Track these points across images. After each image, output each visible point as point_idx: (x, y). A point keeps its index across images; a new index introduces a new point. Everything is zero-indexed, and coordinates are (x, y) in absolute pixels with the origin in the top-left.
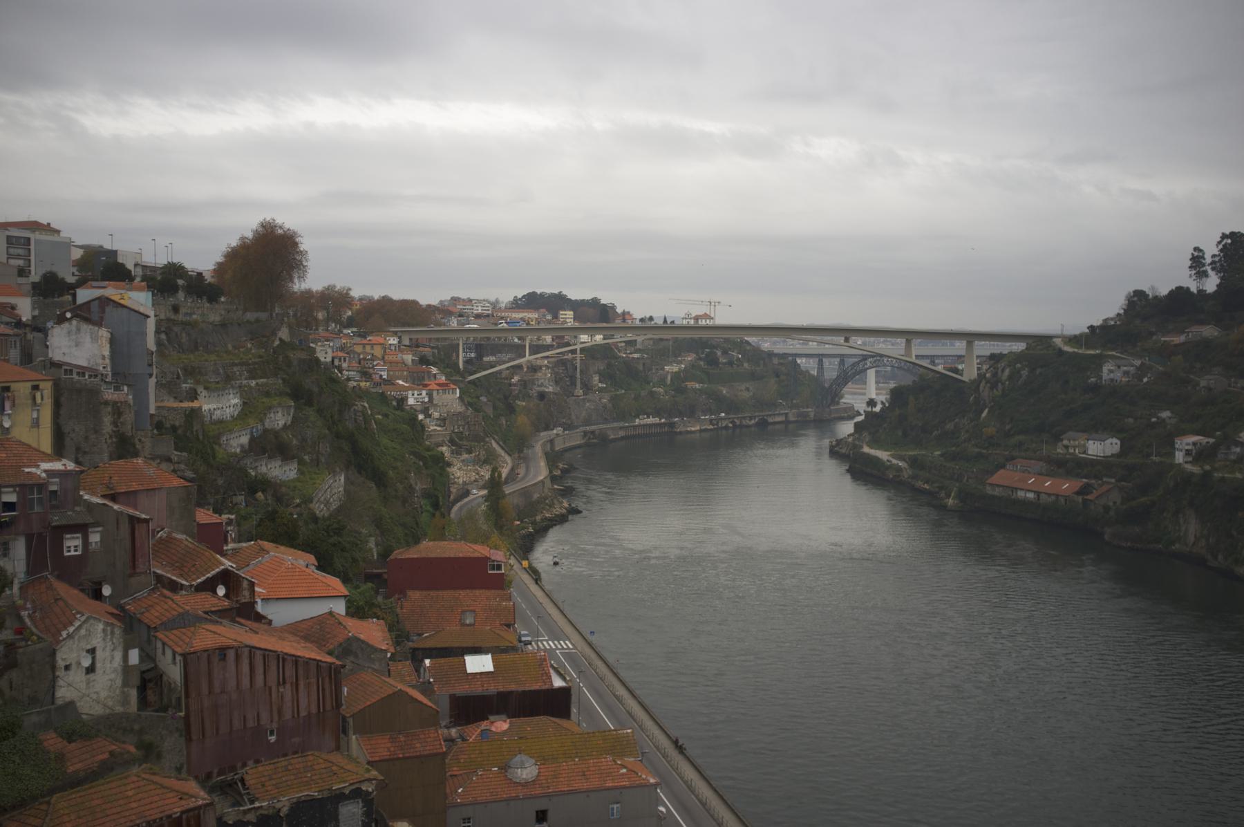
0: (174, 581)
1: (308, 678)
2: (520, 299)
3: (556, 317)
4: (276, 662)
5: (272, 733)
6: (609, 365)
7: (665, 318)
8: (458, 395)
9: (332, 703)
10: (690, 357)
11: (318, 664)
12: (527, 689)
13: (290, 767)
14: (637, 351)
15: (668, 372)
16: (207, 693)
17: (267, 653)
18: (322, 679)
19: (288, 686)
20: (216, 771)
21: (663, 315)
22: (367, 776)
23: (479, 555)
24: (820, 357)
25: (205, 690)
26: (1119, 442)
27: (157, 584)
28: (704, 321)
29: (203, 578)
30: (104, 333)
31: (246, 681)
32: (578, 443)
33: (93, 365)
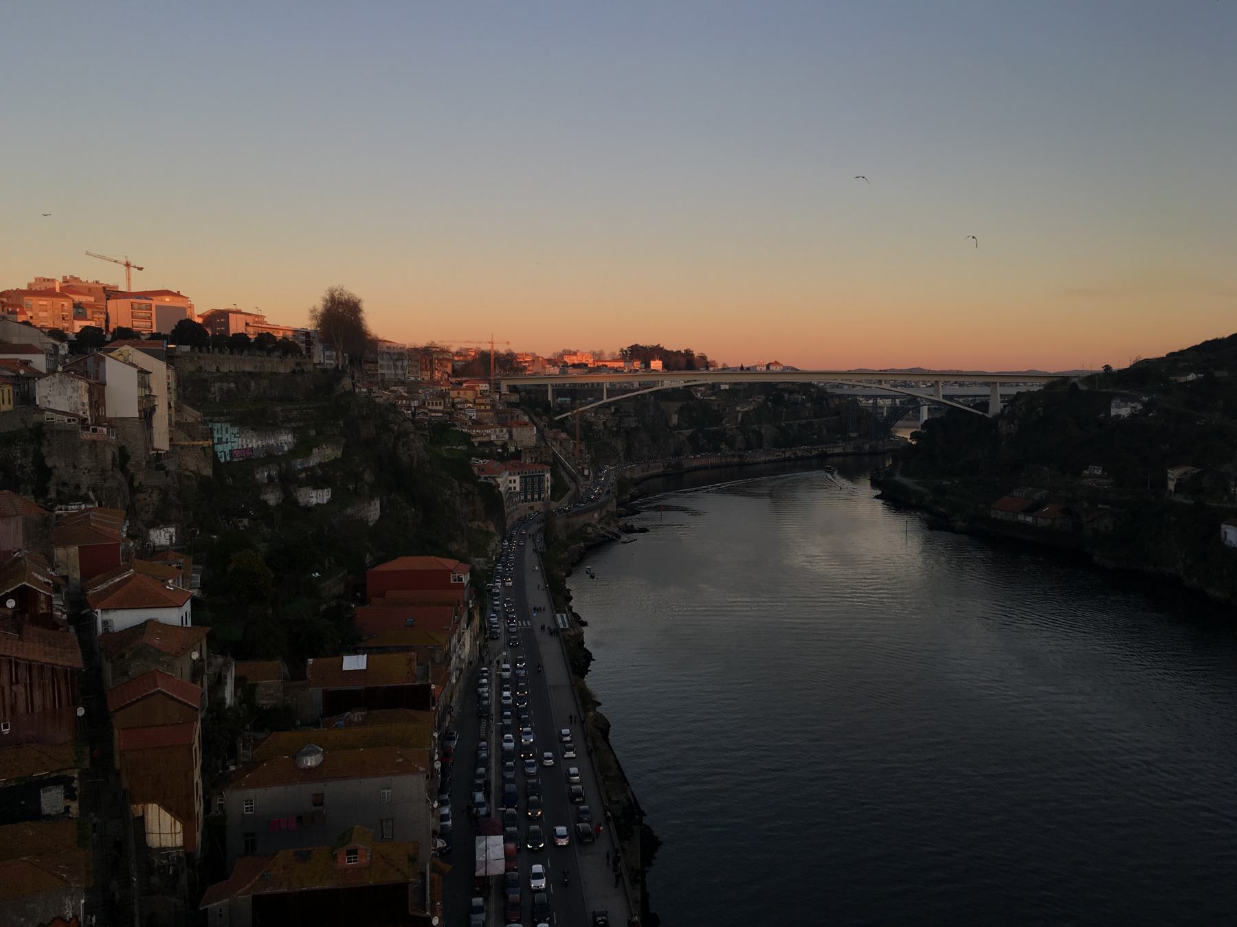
1: (42, 679)
3: (647, 366)
5: (5, 727)
9: (69, 700)
10: (760, 399)
11: (53, 668)
12: (391, 685)
14: (713, 394)
15: (739, 411)
18: (58, 682)
21: (740, 366)
23: (445, 568)
24: (875, 397)
28: (774, 367)
29: (3, 594)
30: (83, 384)
32: (656, 471)
33: (74, 411)
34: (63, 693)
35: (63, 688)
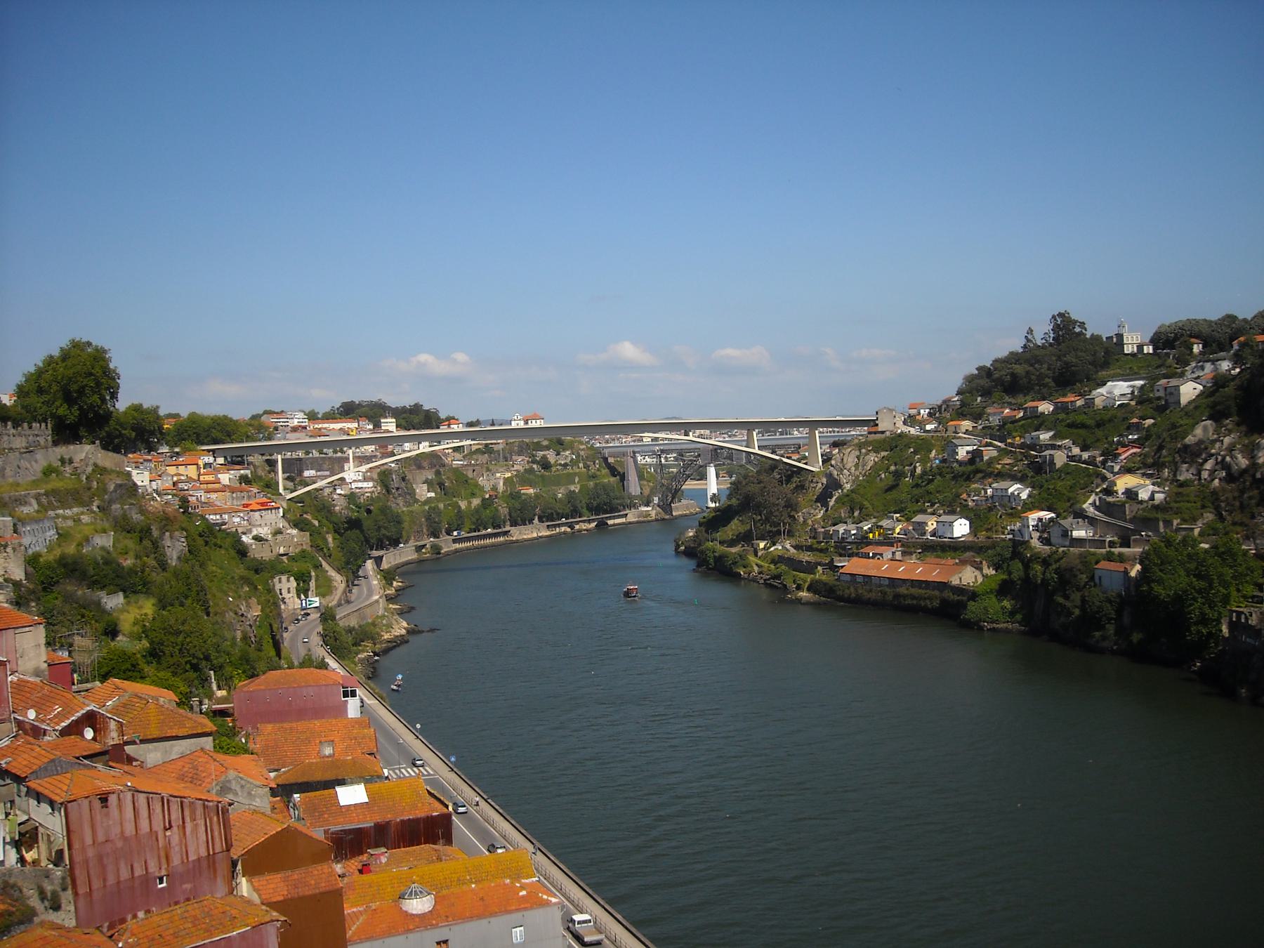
0: (37, 726)
1: (195, 820)
2: (338, 409)
3: (377, 425)
4: (161, 803)
6: (438, 473)
7: (493, 420)
8: (282, 515)
11: (204, 805)
13: (186, 915)
15: (499, 478)
16: (91, 842)
17: (151, 795)
18: (211, 820)
19: (175, 829)
20: (106, 924)
22: (267, 919)
25: (89, 841)
26: (968, 523)
27: (18, 731)
28: (534, 421)
31: (129, 829)
34: (216, 833)
35: (216, 827)
